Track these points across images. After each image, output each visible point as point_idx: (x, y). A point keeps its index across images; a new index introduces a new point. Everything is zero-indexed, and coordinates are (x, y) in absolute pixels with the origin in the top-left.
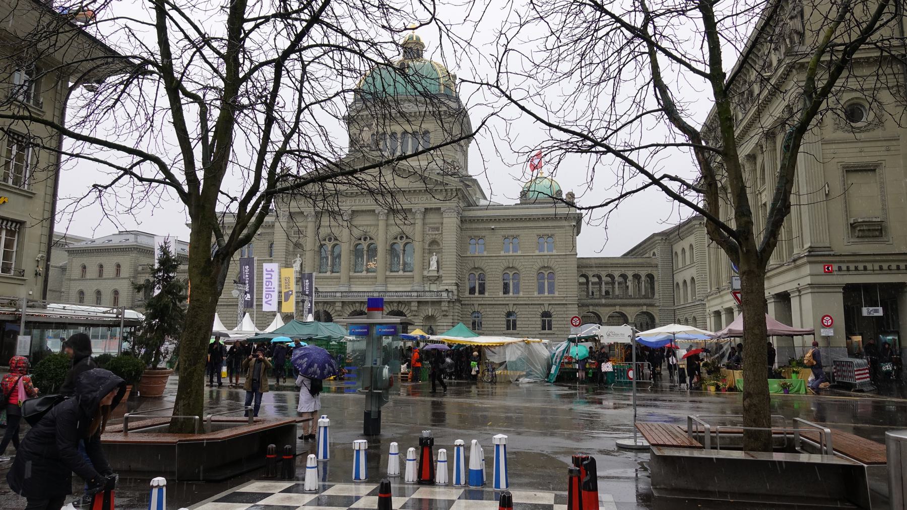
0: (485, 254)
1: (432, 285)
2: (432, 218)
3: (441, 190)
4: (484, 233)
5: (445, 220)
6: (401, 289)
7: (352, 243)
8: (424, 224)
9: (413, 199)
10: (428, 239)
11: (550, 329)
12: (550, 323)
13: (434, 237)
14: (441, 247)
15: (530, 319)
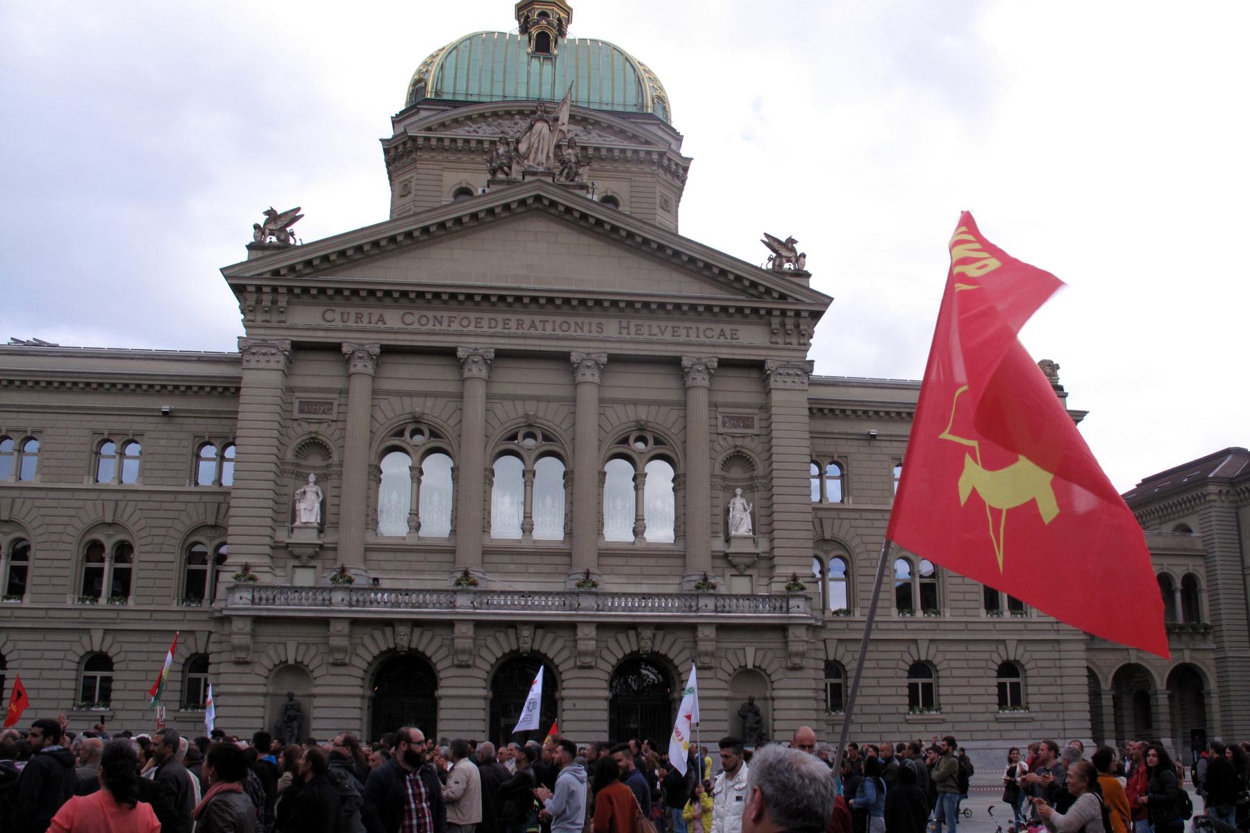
0: (849, 503)
1: (734, 579)
2: (739, 390)
3: (769, 312)
4: (844, 447)
5: (776, 397)
6: (644, 589)
7: (489, 449)
8: (714, 405)
9: (683, 332)
10: (725, 448)
11: (1016, 703)
12: (1015, 687)
13: (739, 442)
14: (760, 469)
15: (973, 681)
